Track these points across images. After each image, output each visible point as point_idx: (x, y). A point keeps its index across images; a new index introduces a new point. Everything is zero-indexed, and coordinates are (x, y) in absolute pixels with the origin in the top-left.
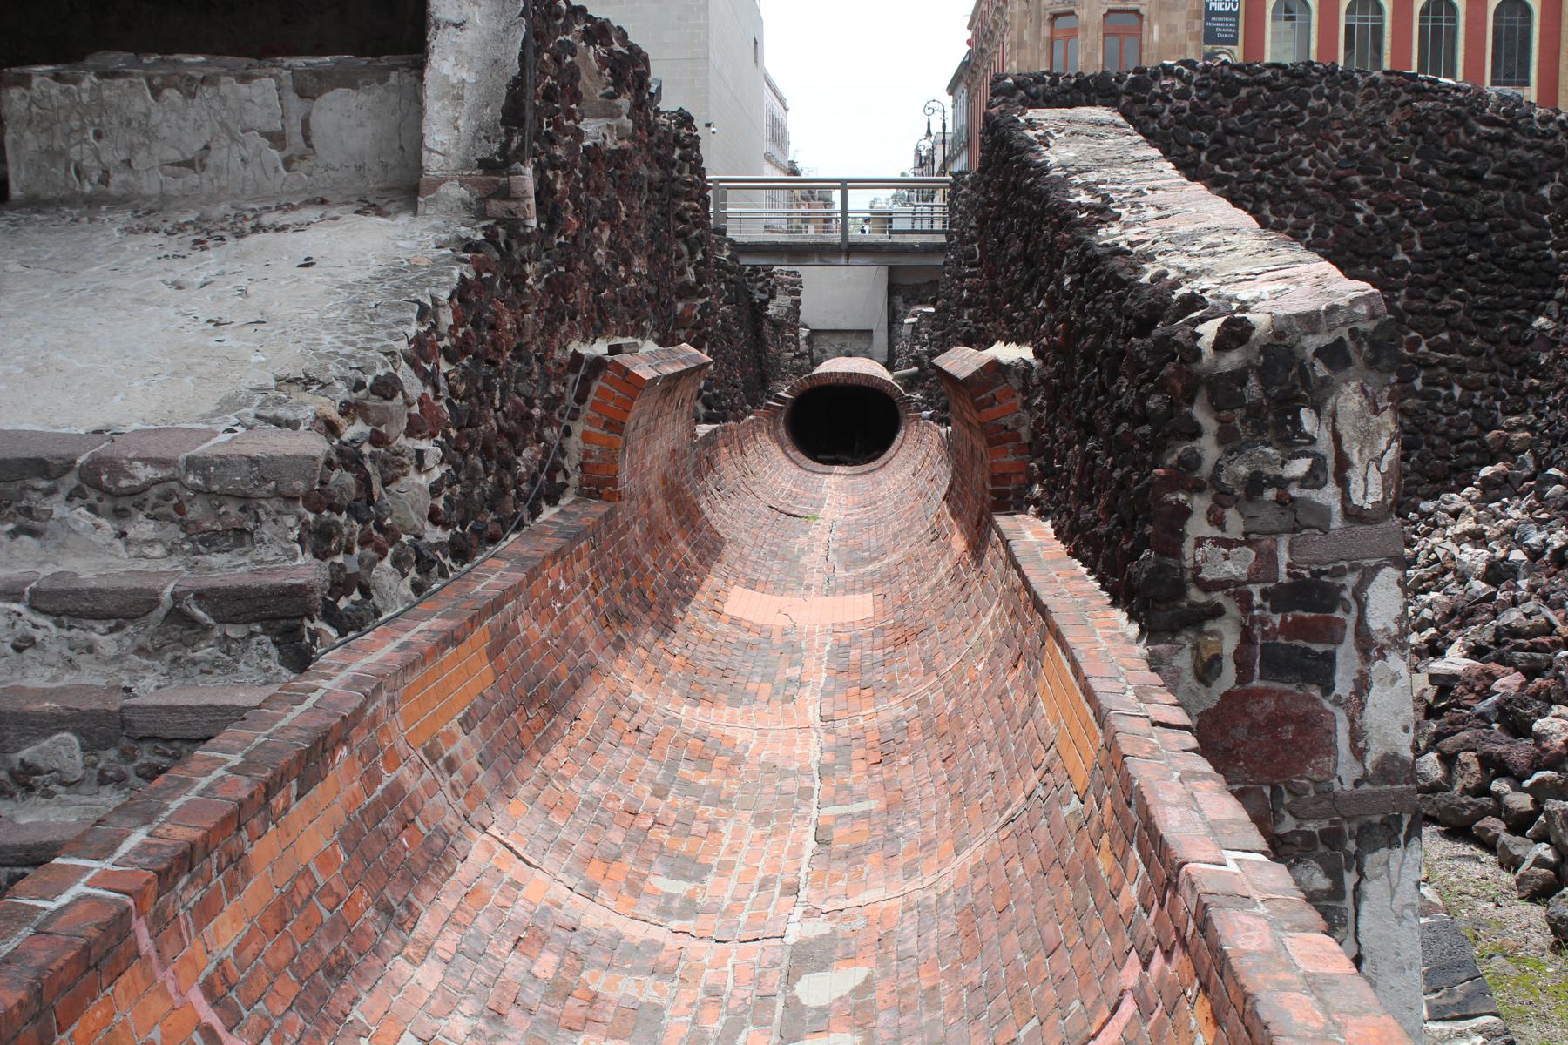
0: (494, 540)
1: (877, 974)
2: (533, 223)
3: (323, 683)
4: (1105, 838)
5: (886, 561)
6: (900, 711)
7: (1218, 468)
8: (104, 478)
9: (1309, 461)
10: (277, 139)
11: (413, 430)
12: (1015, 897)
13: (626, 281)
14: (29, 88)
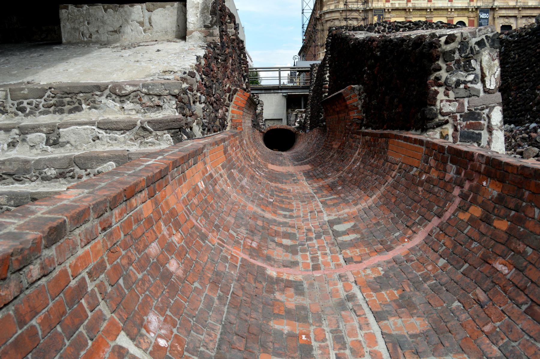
6: (333, 180)
7: (447, 78)
8: (117, 90)
9: (474, 75)
14: (68, 9)
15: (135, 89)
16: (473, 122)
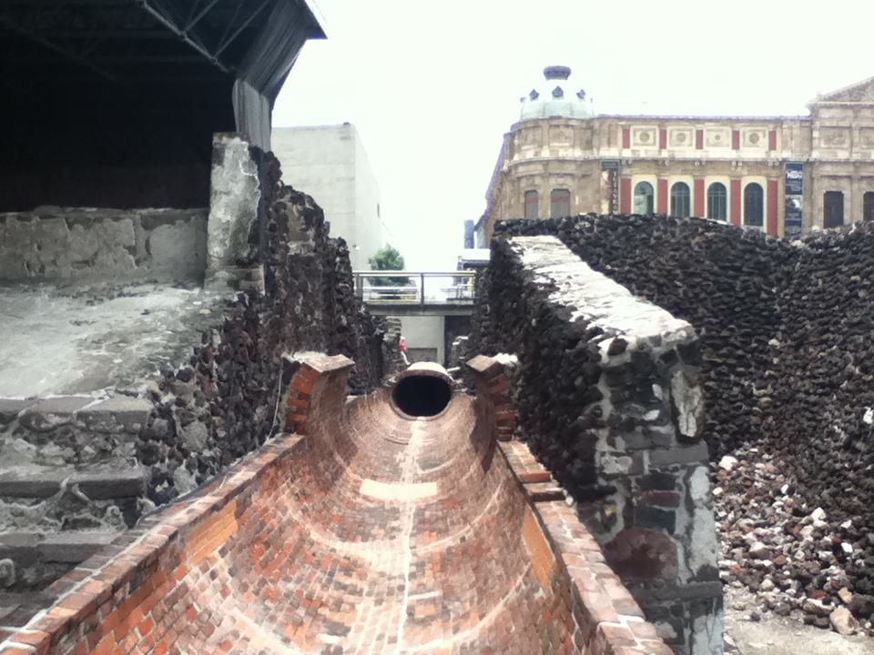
0: (240, 455)
2: (263, 293)
8: (33, 423)
10: (132, 250)
13: (311, 322)
15: (64, 420)
16: (659, 492)
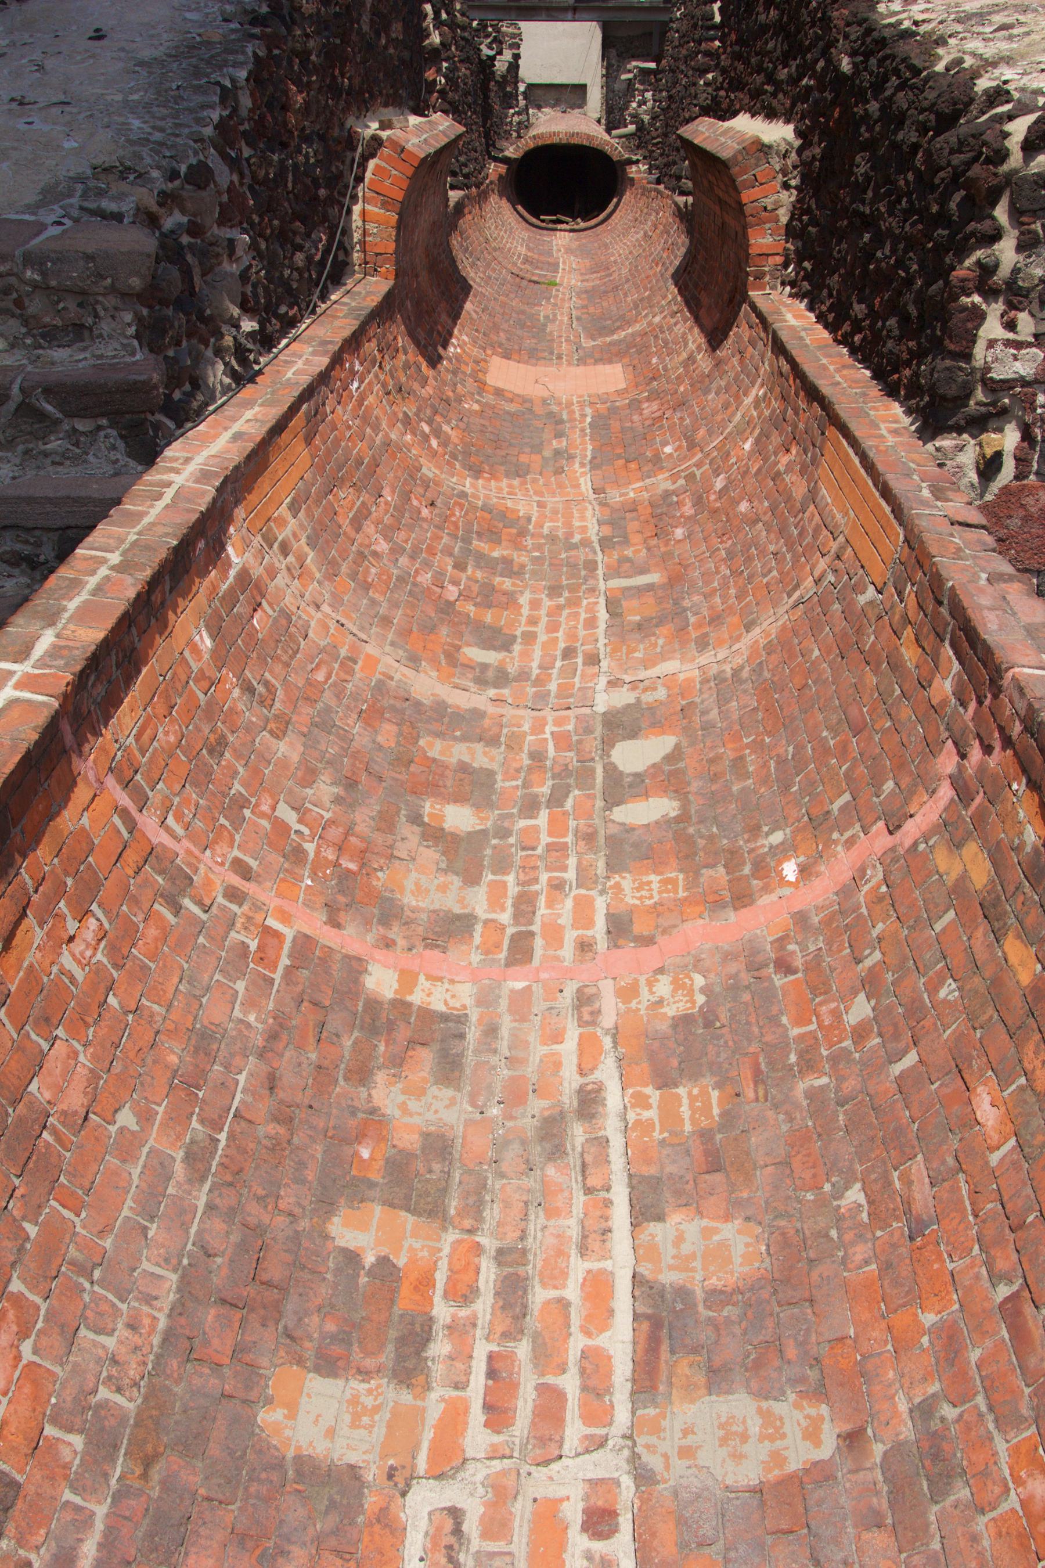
1: (684, 744)
3: (172, 476)
4: (908, 633)
5: (630, 331)
6: (669, 485)
7: (1016, 271)
11: (224, 220)
12: (814, 676)
13: (386, 48)
